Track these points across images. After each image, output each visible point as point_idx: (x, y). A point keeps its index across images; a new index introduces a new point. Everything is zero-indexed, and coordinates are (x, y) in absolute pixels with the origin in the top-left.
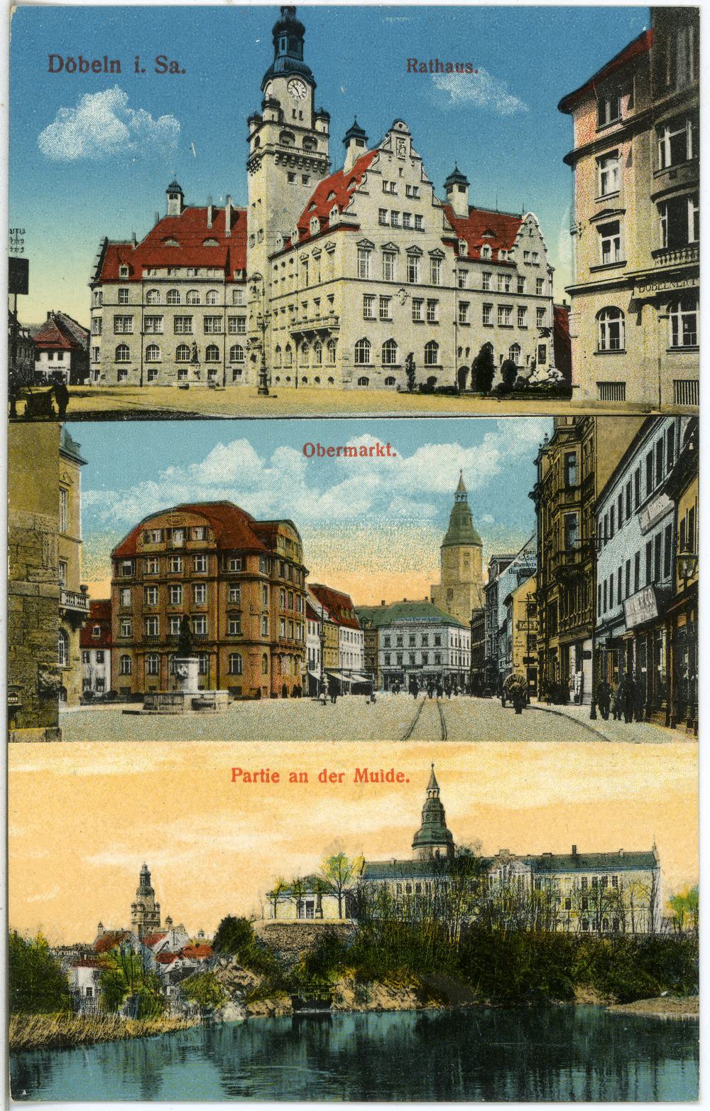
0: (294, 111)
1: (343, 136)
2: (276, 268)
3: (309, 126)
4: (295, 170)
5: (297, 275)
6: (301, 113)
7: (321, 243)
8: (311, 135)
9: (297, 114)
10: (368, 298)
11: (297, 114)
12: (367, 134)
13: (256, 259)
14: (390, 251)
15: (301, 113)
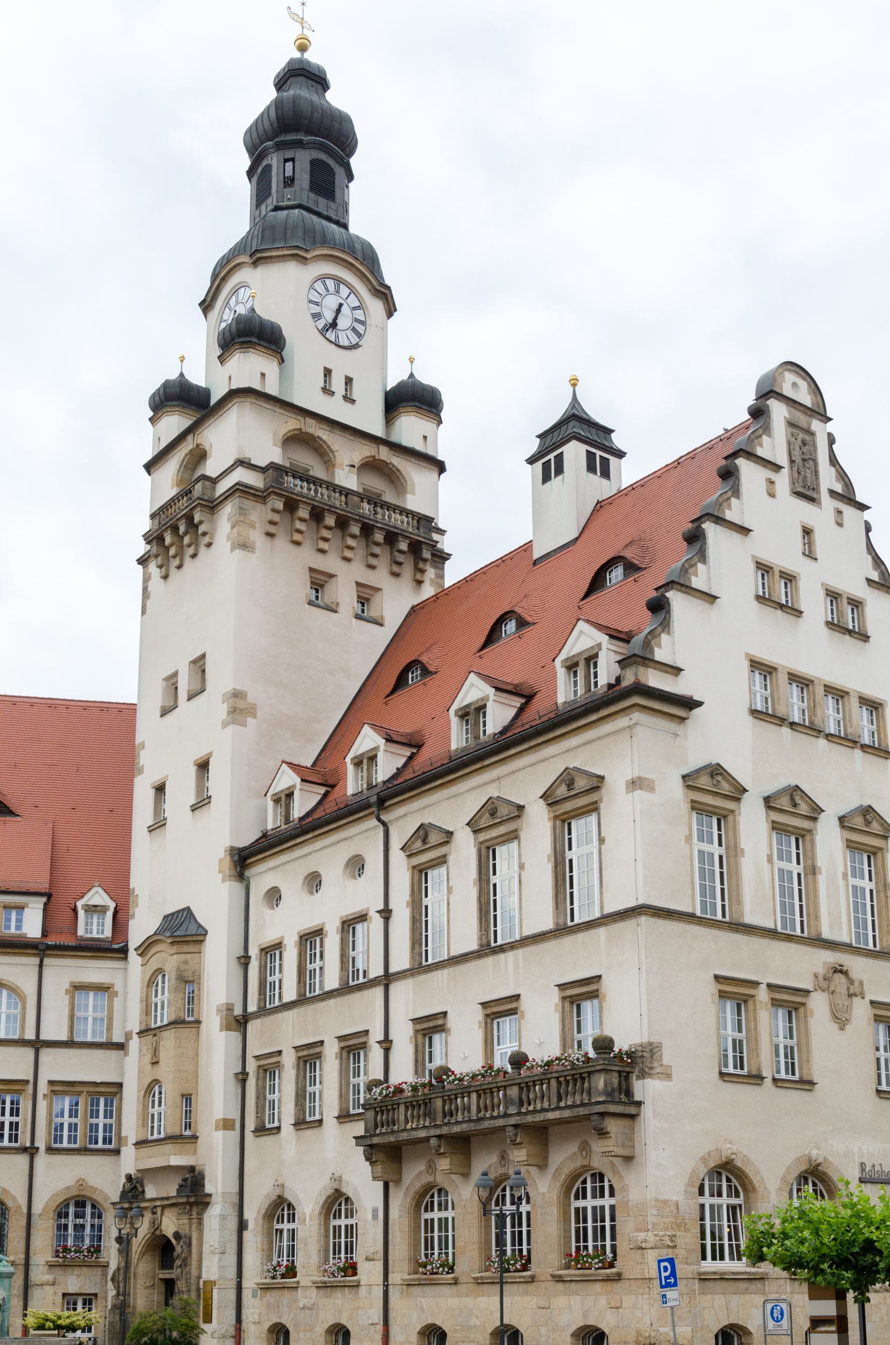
0: (328, 372)
1: (534, 446)
2: (274, 896)
3: (376, 428)
4: (331, 563)
5: (386, 913)
6: (349, 381)
7: (524, 781)
8: (384, 454)
9: (338, 385)
10: (735, 992)
11: (338, 385)
12: (617, 440)
13: (176, 866)
14: (793, 813)
15: (349, 381)
